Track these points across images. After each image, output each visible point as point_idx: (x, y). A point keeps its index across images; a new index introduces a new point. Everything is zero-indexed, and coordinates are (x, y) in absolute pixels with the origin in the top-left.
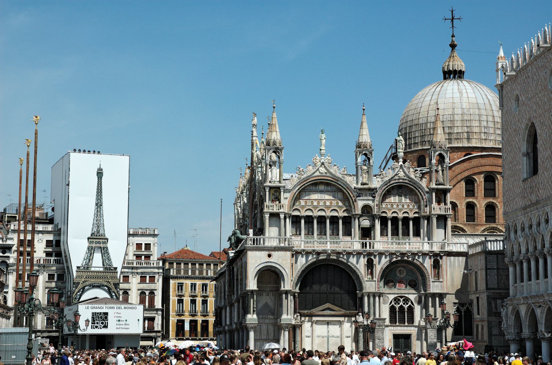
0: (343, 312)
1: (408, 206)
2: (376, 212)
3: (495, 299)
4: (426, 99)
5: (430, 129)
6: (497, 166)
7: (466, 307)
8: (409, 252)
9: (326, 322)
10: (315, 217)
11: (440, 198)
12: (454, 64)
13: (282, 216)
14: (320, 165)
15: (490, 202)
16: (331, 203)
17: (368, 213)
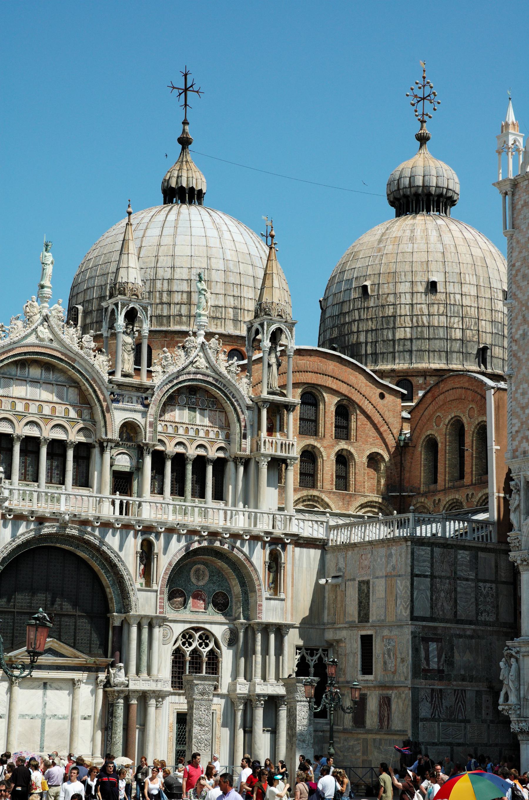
0: (83, 659)
1: (207, 432)
2: (149, 440)
3: (426, 640)
4: (149, 233)
5: (161, 293)
6: (326, 375)
7: (318, 655)
8: (226, 530)
9: (42, 683)
10: (18, 437)
11: (272, 423)
12: (190, 175)
14: (39, 321)
15: (309, 445)
16: (54, 409)
17: (129, 439)
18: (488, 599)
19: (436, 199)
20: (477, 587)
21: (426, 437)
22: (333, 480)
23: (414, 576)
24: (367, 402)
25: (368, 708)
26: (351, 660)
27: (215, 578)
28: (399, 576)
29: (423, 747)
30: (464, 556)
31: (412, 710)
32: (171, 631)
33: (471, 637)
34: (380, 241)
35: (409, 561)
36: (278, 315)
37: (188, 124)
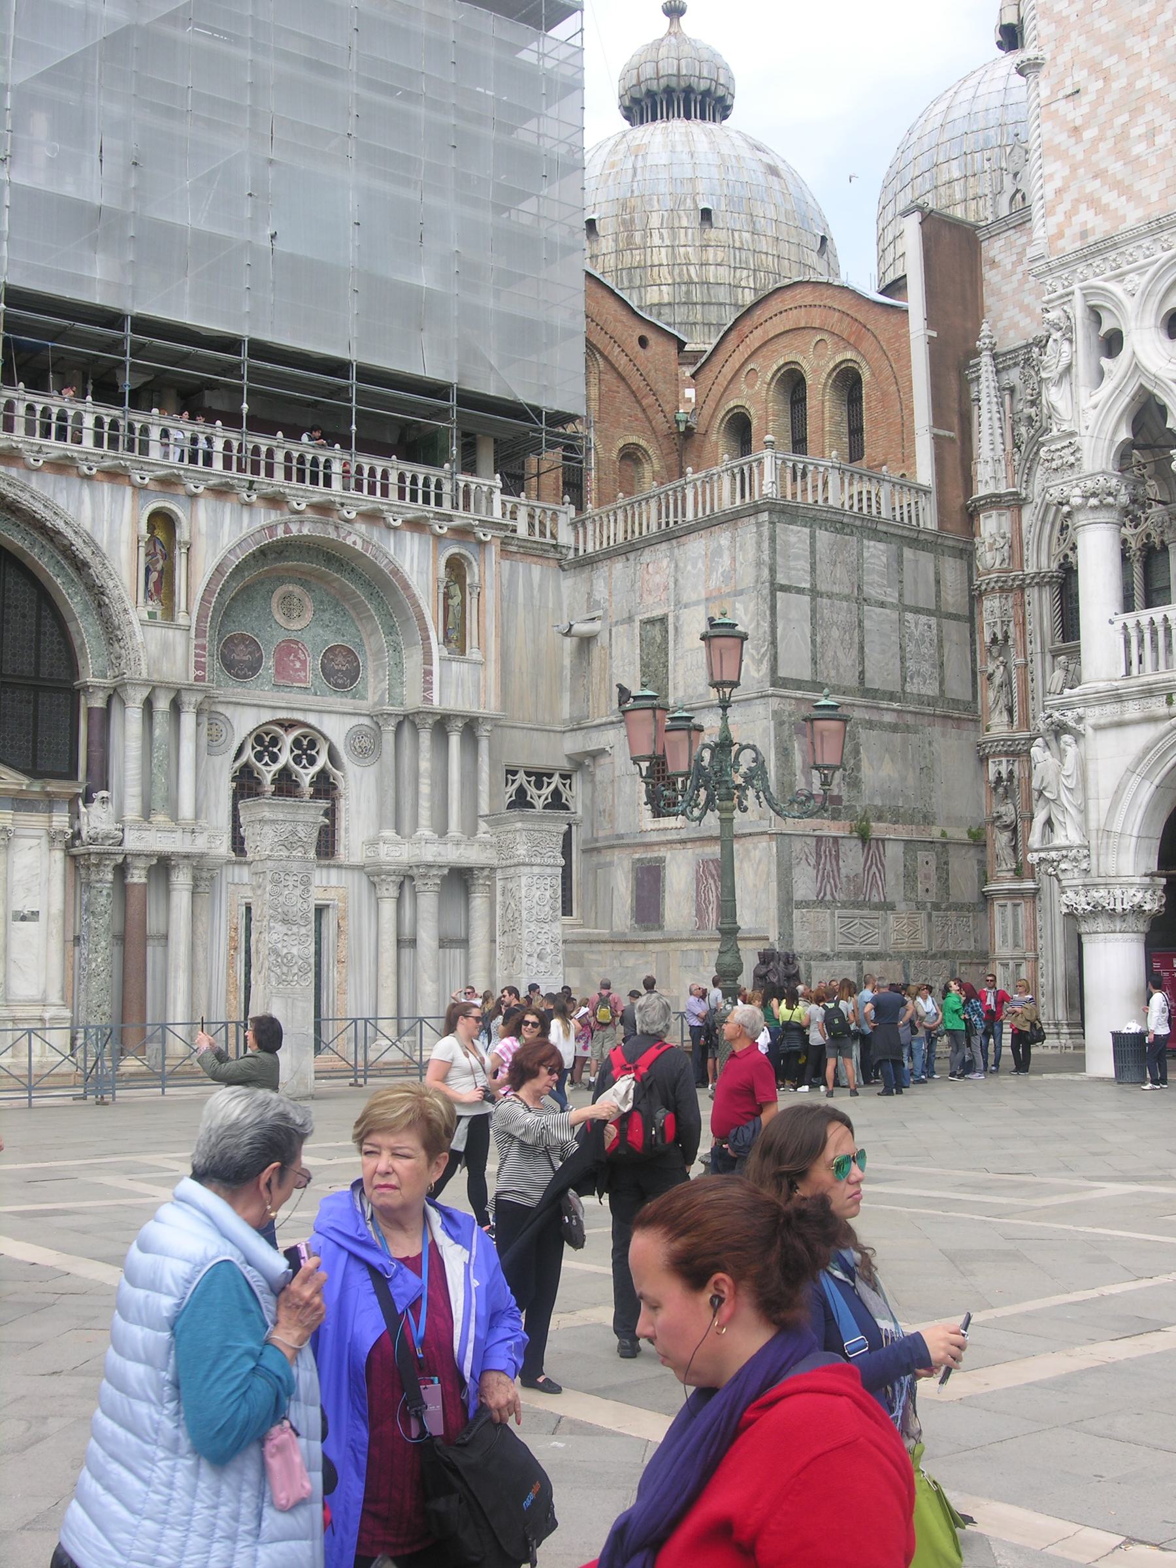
7: (552, 787)
18: (924, 650)
19: (699, 98)
20: (901, 621)
21: (728, 412)
22: (558, 488)
23: (776, 590)
25: (667, 887)
26: (627, 790)
27: (326, 616)
28: (741, 593)
29: (801, 964)
30: (876, 553)
31: (779, 883)
32: (228, 726)
33: (894, 728)
35: (766, 557)
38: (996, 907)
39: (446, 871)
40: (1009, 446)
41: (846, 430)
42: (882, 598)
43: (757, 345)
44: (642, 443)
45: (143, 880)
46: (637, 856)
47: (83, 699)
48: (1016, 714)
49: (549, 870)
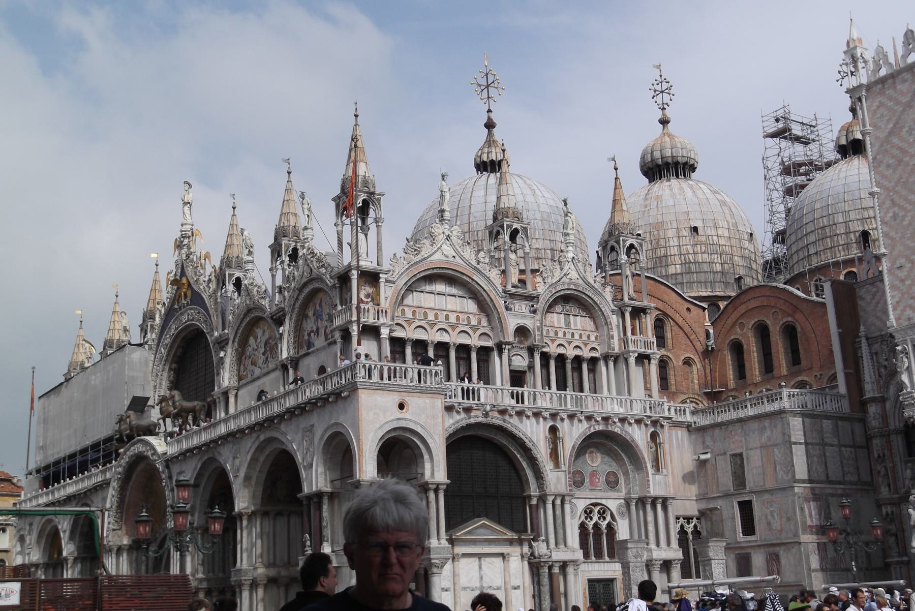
0: (510, 535)
1: (581, 336)
7: (693, 524)
10: (432, 342)
13: (385, 332)
16: (458, 318)
17: (520, 342)
20: (840, 451)
21: (731, 341)
24: (678, 315)
28: (776, 445)
34: (646, 199)
36: (630, 233)
37: (492, 112)
38: (892, 569)
39: (662, 562)
40: (877, 377)
41: (790, 351)
42: (832, 443)
43: (743, 312)
44: (692, 356)
45: (558, 571)
46: (737, 552)
47: (527, 501)
48: (892, 487)
49: (721, 561)
